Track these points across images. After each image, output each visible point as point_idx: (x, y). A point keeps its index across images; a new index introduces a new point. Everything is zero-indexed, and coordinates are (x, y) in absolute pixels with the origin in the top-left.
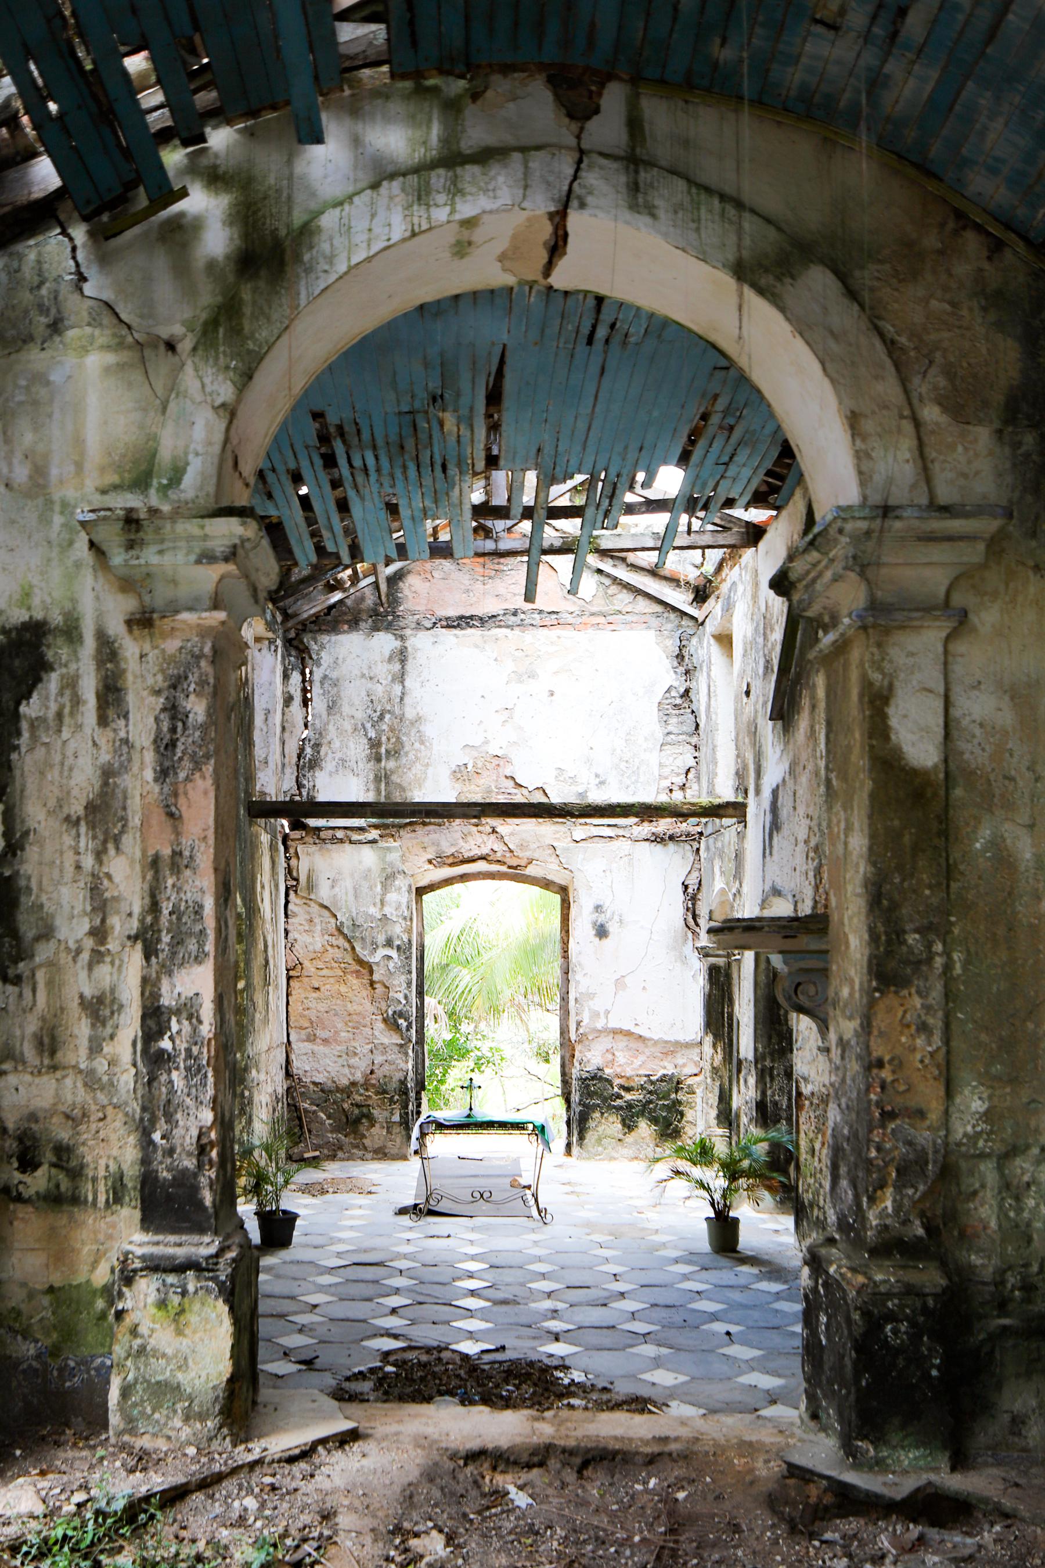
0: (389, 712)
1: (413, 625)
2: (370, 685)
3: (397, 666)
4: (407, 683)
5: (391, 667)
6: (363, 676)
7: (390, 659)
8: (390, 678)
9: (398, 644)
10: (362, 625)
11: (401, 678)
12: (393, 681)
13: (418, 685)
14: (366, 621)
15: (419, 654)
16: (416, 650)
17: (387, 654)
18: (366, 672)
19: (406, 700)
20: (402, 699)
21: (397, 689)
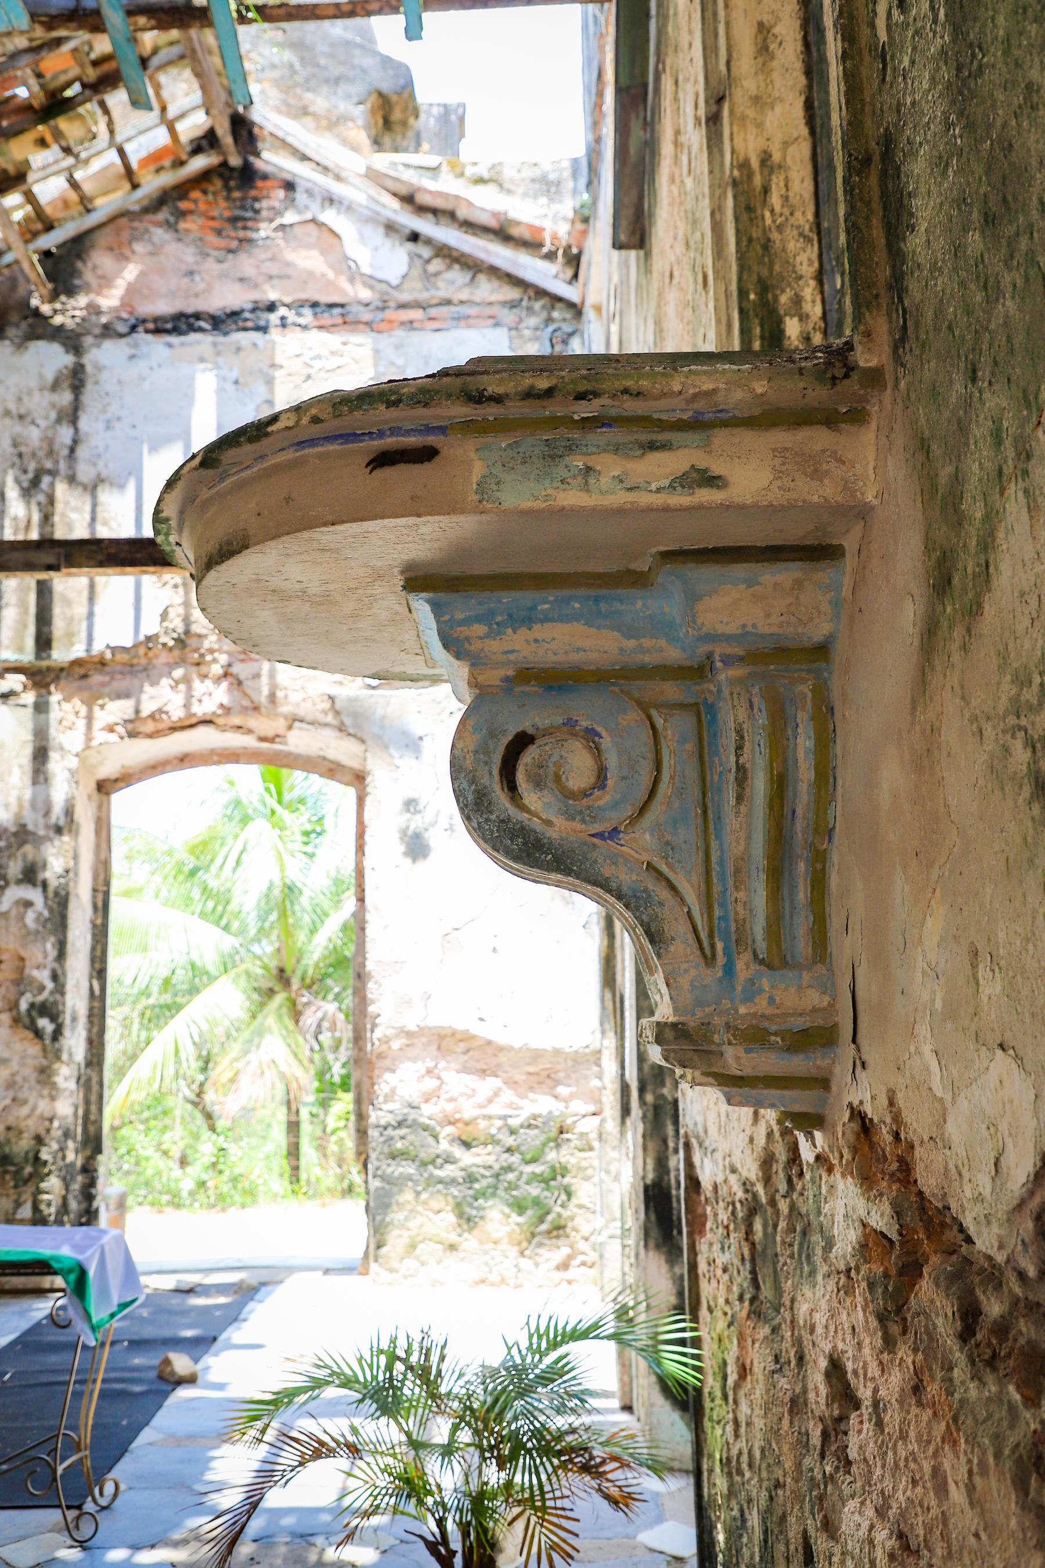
0: (50, 472)
1: (97, 331)
2: (18, 428)
3: (66, 397)
4: (83, 423)
5: (55, 398)
6: (7, 413)
7: (55, 386)
8: (53, 415)
9: (69, 360)
10: (11, 332)
11: (72, 415)
12: (59, 421)
13: (101, 426)
14: (17, 326)
15: (104, 376)
16: (99, 368)
17: (50, 377)
18: (12, 407)
19: (82, 452)
20: (72, 450)
21: (65, 434)
